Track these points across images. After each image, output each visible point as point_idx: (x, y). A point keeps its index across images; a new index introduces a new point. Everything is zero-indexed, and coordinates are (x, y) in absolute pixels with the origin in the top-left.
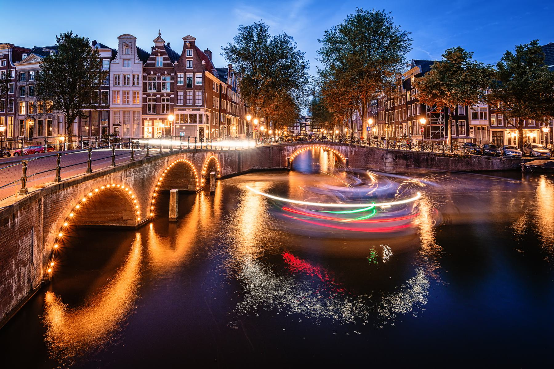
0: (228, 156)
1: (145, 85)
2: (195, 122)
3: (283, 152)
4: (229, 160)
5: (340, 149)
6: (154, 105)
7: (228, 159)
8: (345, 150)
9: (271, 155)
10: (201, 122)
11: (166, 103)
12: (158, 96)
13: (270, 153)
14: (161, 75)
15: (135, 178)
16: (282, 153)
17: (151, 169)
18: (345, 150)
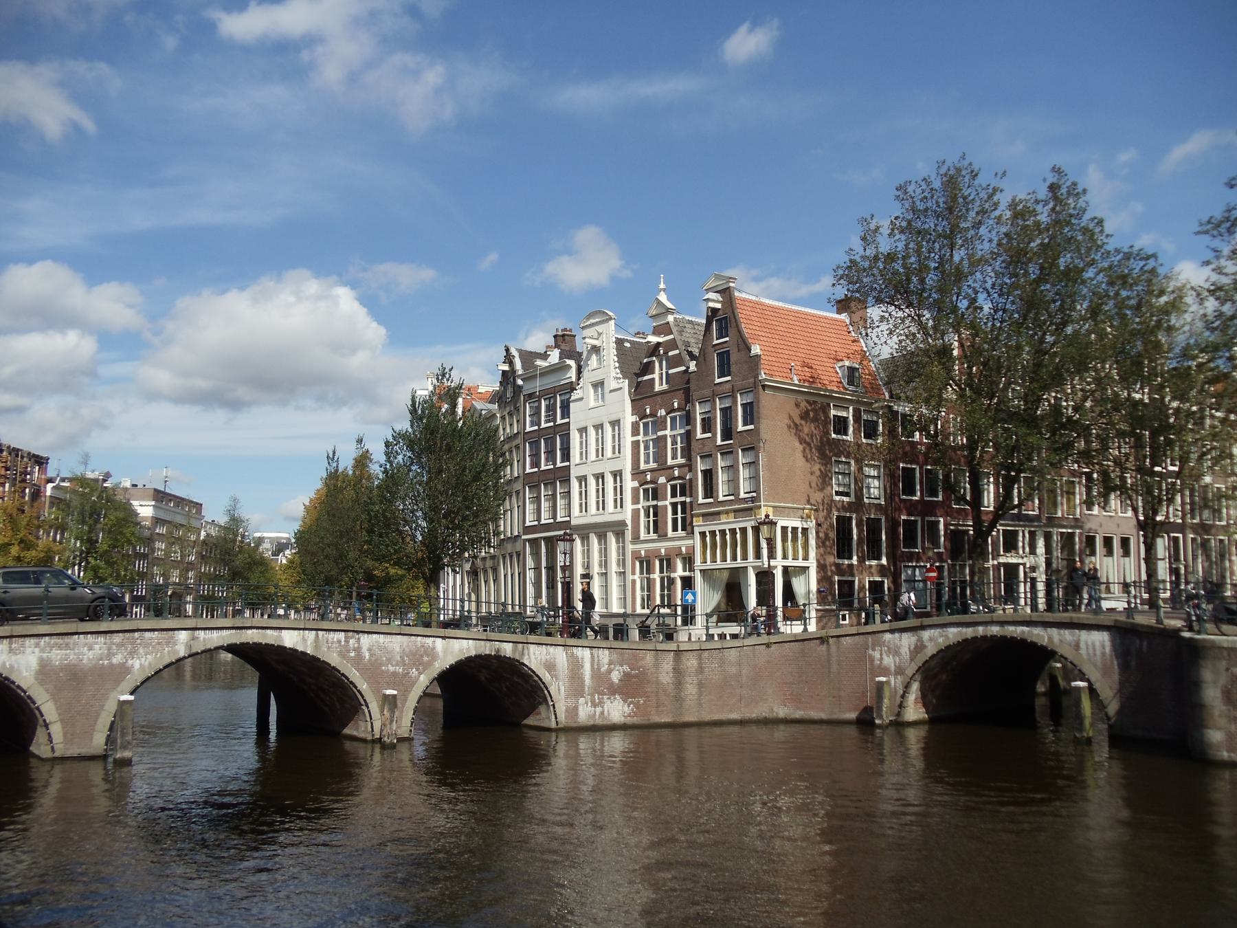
0: (610, 663)
1: (636, 445)
2: (745, 557)
3: (877, 655)
4: (615, 677)
5: (1082, 645)
6: (655, 507)
7: (609, 671)
8: (1103, 647)
9: (834, 668)
10: (758, 555)
11: (679, 499)
12: (662, 480)
13: (829, 661)
14: (667, 414)
15: (41, 660)
16: (872, 660)
17: (109, 649)
18: (1103, 647)
